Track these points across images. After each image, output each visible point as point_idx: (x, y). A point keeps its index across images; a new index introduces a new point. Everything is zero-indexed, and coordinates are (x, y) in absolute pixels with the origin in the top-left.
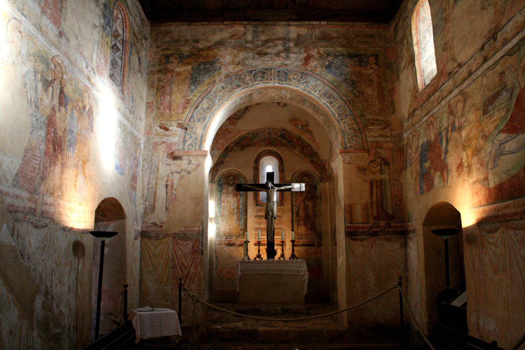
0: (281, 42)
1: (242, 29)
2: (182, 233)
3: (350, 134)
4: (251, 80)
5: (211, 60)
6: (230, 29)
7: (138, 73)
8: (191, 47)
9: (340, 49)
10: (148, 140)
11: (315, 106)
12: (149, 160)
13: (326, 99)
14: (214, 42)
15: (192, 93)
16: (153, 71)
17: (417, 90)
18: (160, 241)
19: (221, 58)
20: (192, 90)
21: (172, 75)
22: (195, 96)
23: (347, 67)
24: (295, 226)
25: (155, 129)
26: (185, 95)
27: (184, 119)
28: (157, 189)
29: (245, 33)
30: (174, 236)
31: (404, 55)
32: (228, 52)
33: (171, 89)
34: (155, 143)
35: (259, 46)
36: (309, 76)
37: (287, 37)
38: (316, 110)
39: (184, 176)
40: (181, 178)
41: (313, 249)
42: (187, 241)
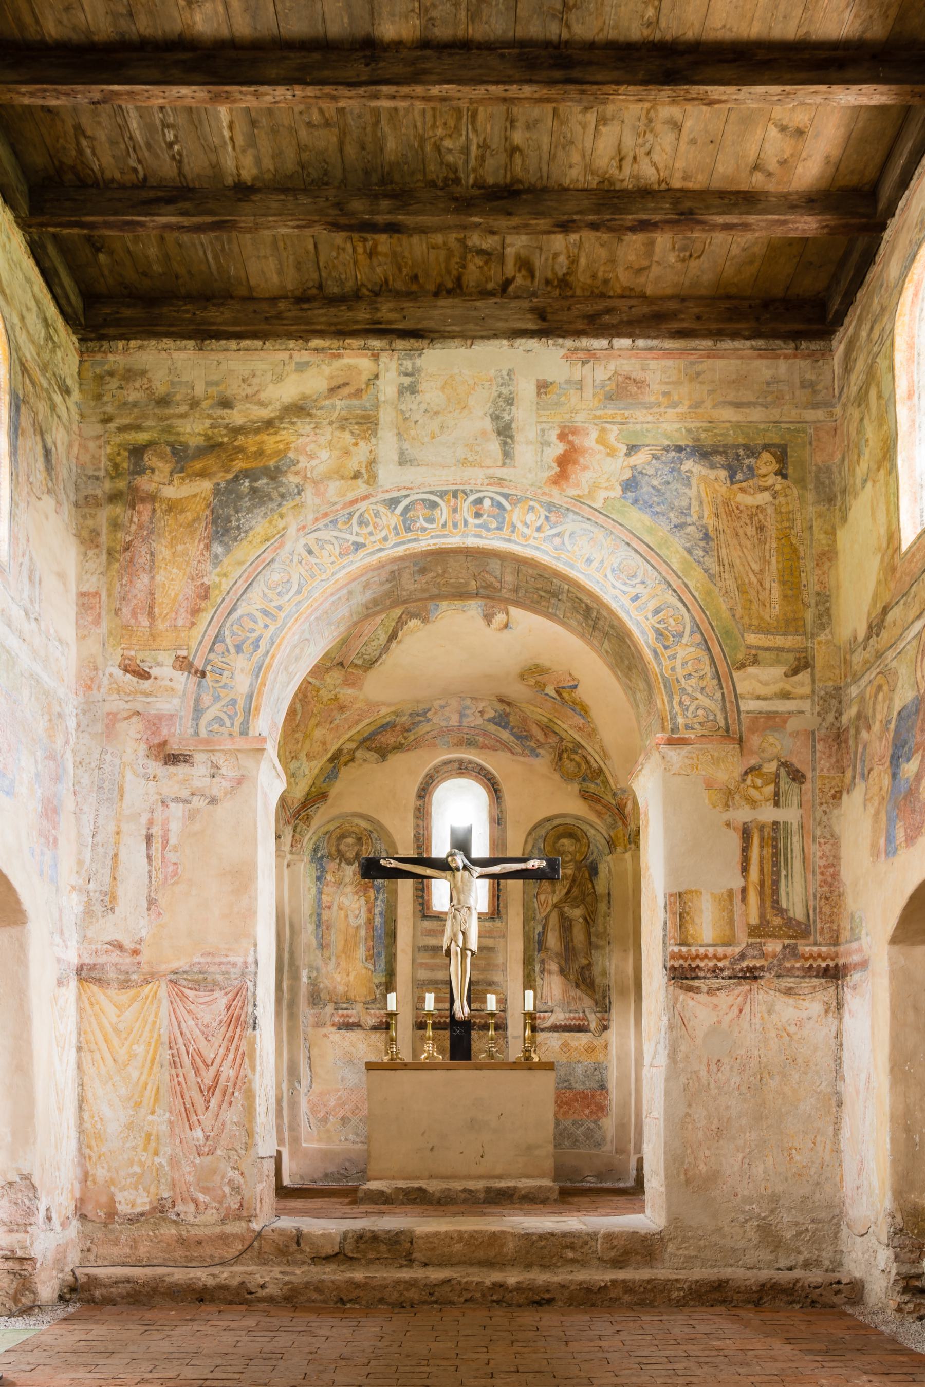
1: (364, 363)
5: (272, 464)
6: (330, 365)
7: (45, 497)
8: (208, 422)
10: (87, 708)
14: (278, 406)
19: (302, 459)
20: (216, 556)
21: (154, 510)
22: (225, 575)
25: (107, 673)
26: (194, 573)
29: (377, 377)
32: (322, 440)
33: (152, 554)
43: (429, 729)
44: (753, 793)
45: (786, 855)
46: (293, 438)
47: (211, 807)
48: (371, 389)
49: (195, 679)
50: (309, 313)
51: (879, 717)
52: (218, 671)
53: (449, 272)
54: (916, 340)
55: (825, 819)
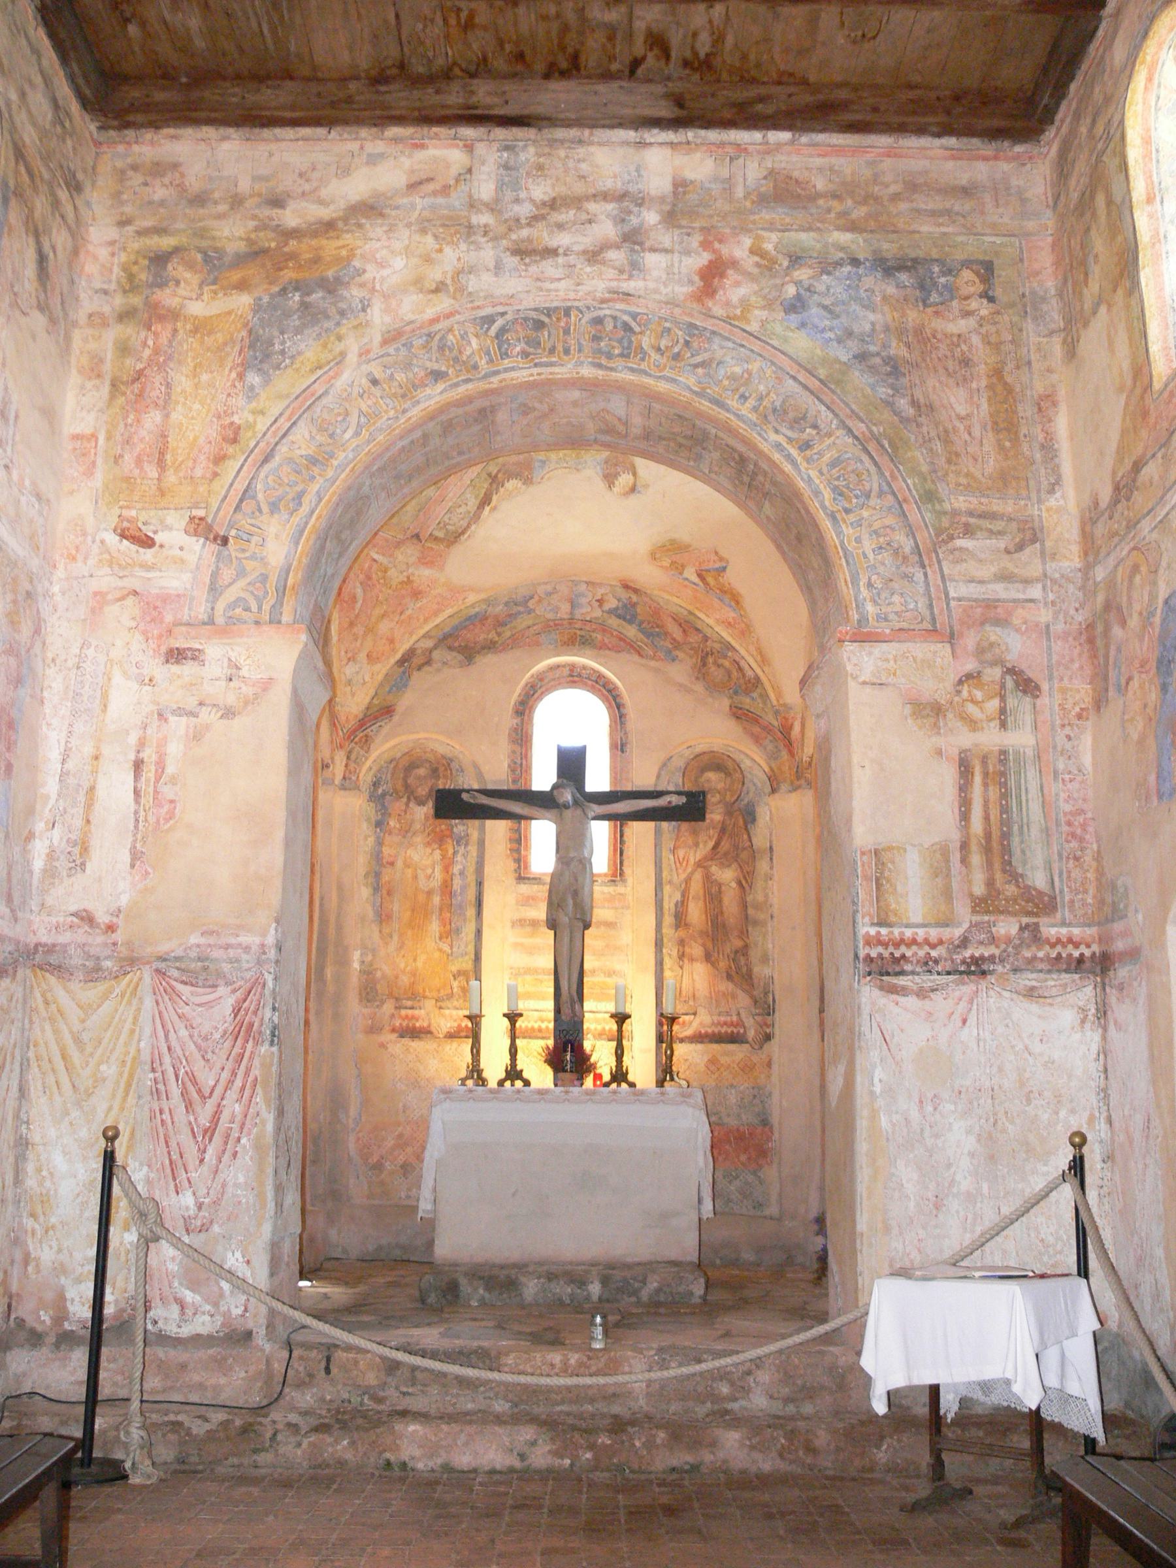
0: (611, 207)
1: (455, 157)
2: (193, 954)
3: (881, 569)
4: (488, 353)
6: (410, 156)
8: (252, 224)
9: (845, 238)
11: (743, 460)
12: (70, 663)
13: (784, 430)
15: (250, 399)
16: (101, 315)
17: (1146, 380)
18: (101, 987)
20: (252, 388)
22: (262, 413)
23: (870, 307)
24: (668, 963)
25: (98, 539)
27: (215, 506)
28: (100, 775)
29: (470, 171)
30: (162, 966)
31: (1096, 256)
32: (397, 245)
33: (168, 385)
34: (96, 594)
35: (523, 221)
36: (717, 340)
37: (632, 188)
38: (746, 479)
39: (207, 727)
40: (197, 736)
41: (738, 1052)
42: (215, 986)
43: (530, 622)
44: (971, 709)
45: (1019, 797)
46: (359, 243)
48: (463, 187)
49: (214, 547)
50: (388, 97)
51: (1137, 607)
52: (245, 537)
53: (563, 49)
54: (1153, 133)
55: (1068, 746)
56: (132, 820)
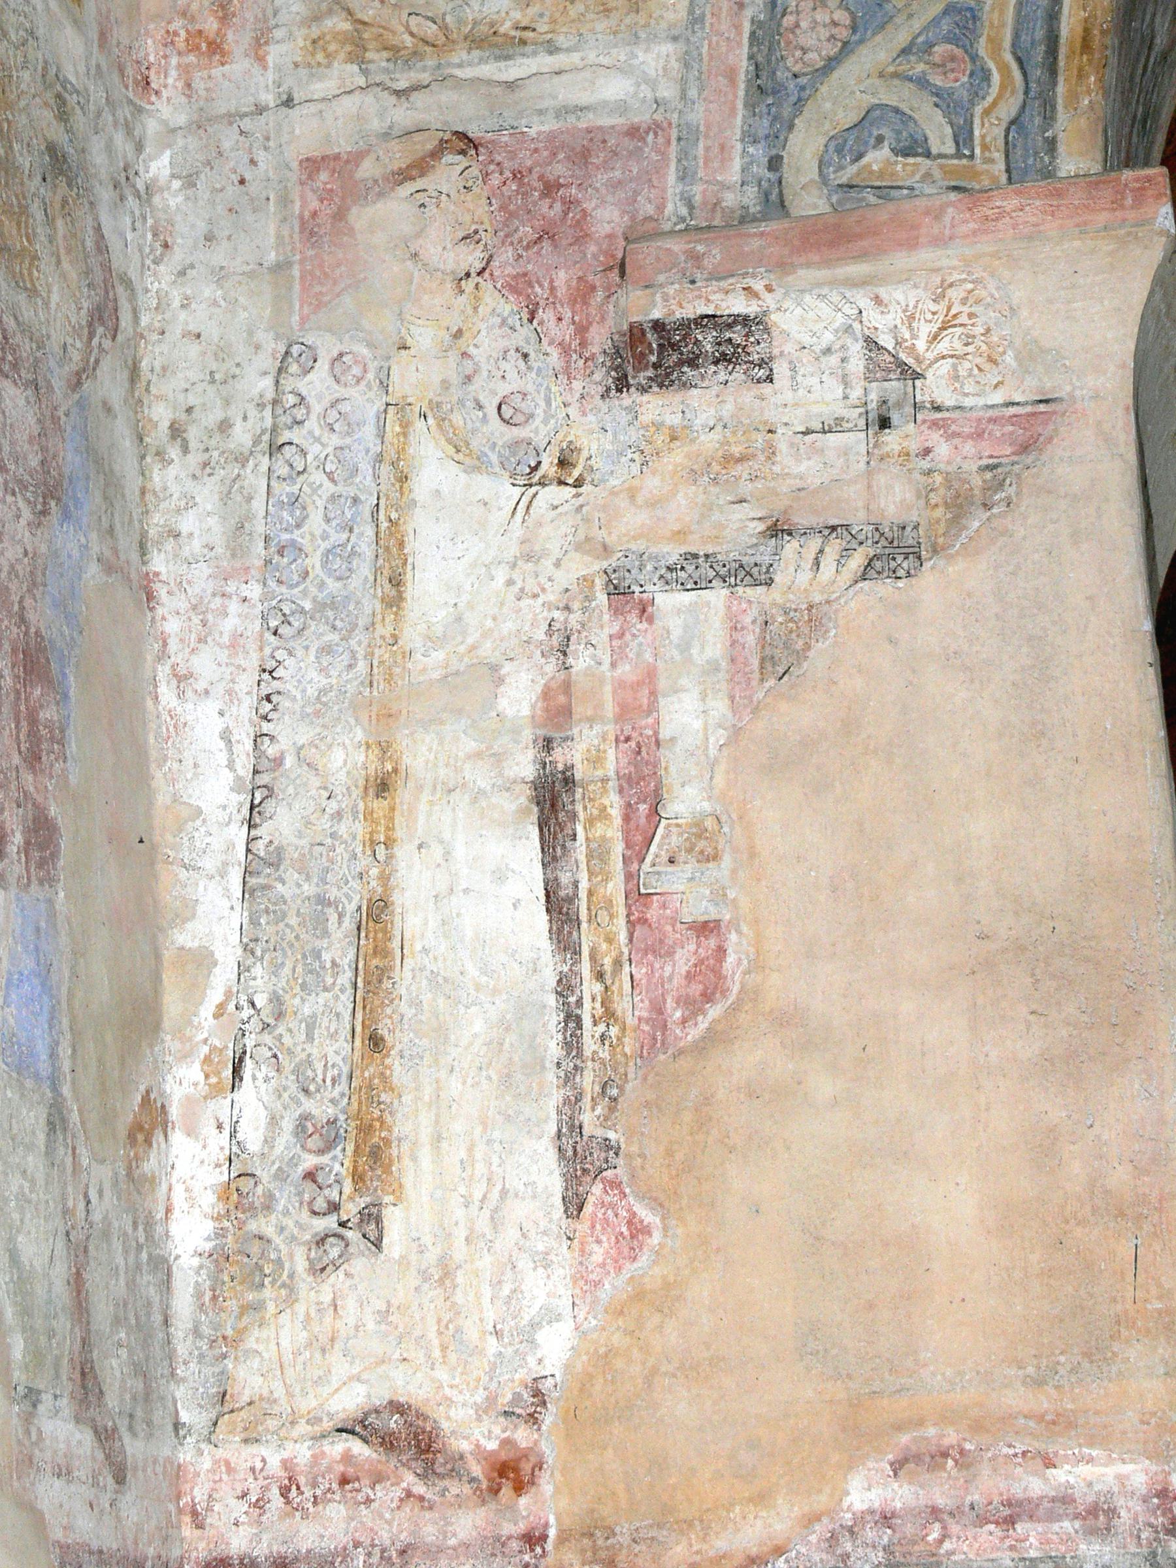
12: (241, 436)
28: (404, 853)
34: (312, 165)
47: (884, 588)
56: (554, 1019)
